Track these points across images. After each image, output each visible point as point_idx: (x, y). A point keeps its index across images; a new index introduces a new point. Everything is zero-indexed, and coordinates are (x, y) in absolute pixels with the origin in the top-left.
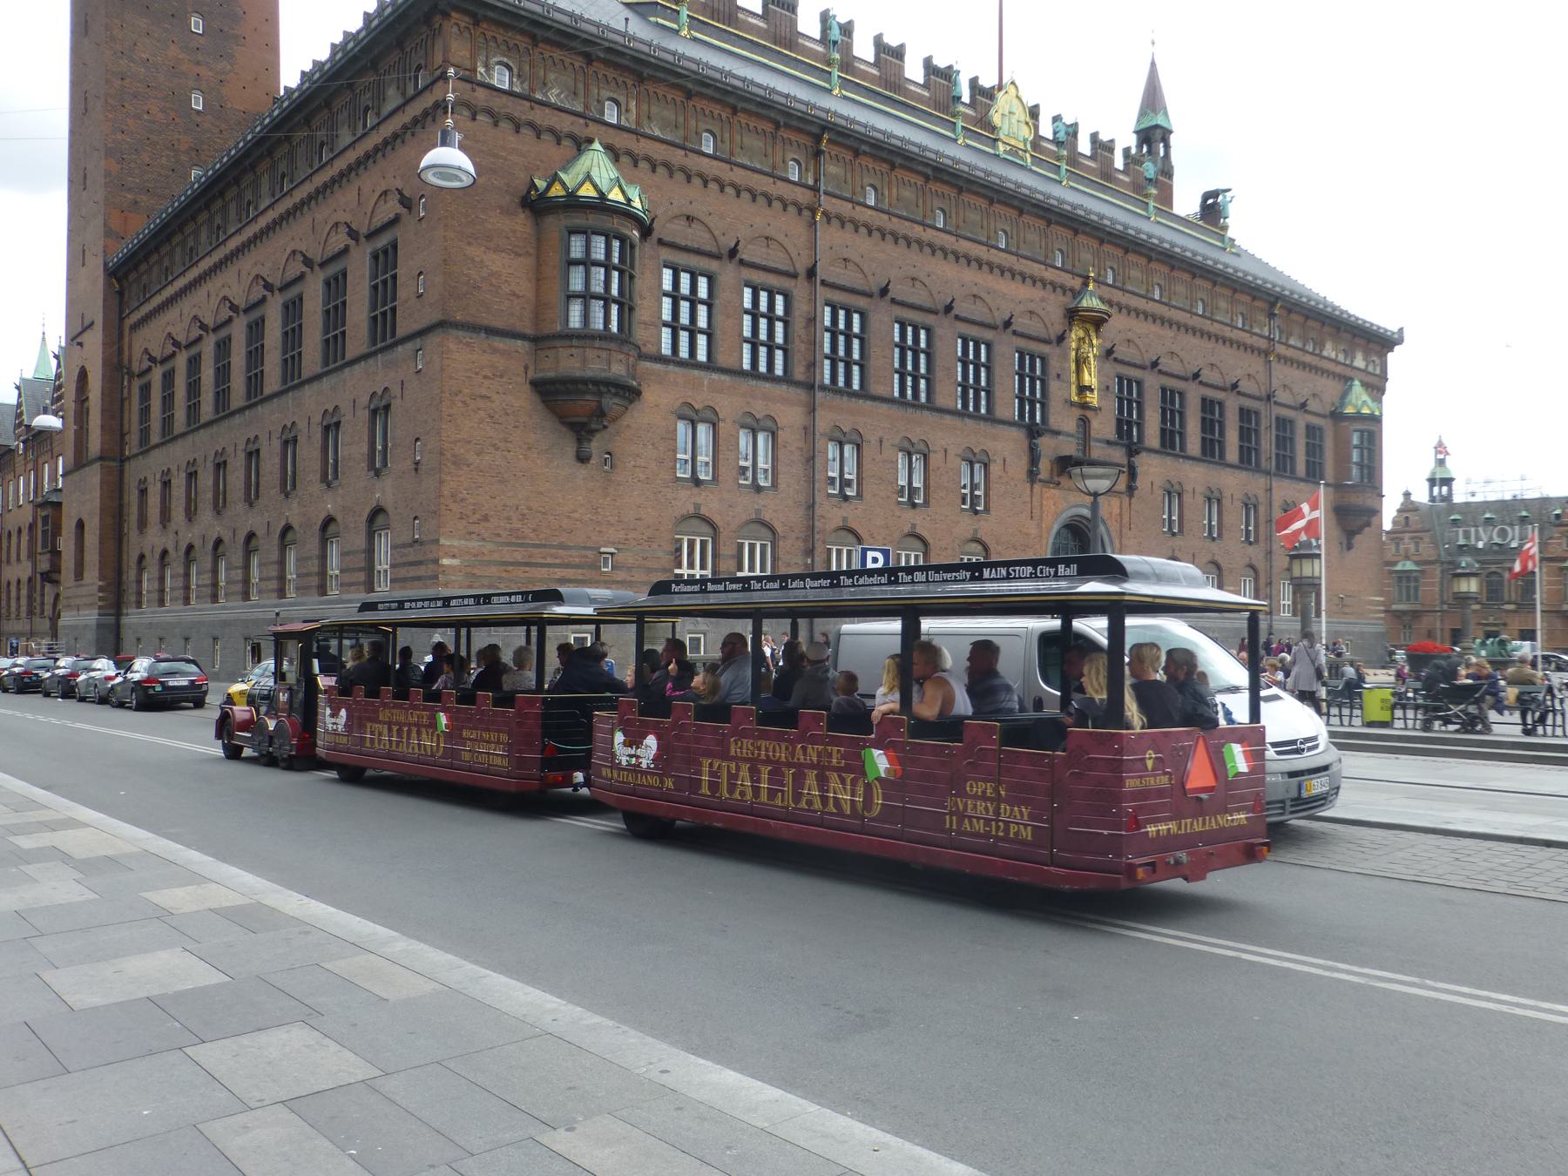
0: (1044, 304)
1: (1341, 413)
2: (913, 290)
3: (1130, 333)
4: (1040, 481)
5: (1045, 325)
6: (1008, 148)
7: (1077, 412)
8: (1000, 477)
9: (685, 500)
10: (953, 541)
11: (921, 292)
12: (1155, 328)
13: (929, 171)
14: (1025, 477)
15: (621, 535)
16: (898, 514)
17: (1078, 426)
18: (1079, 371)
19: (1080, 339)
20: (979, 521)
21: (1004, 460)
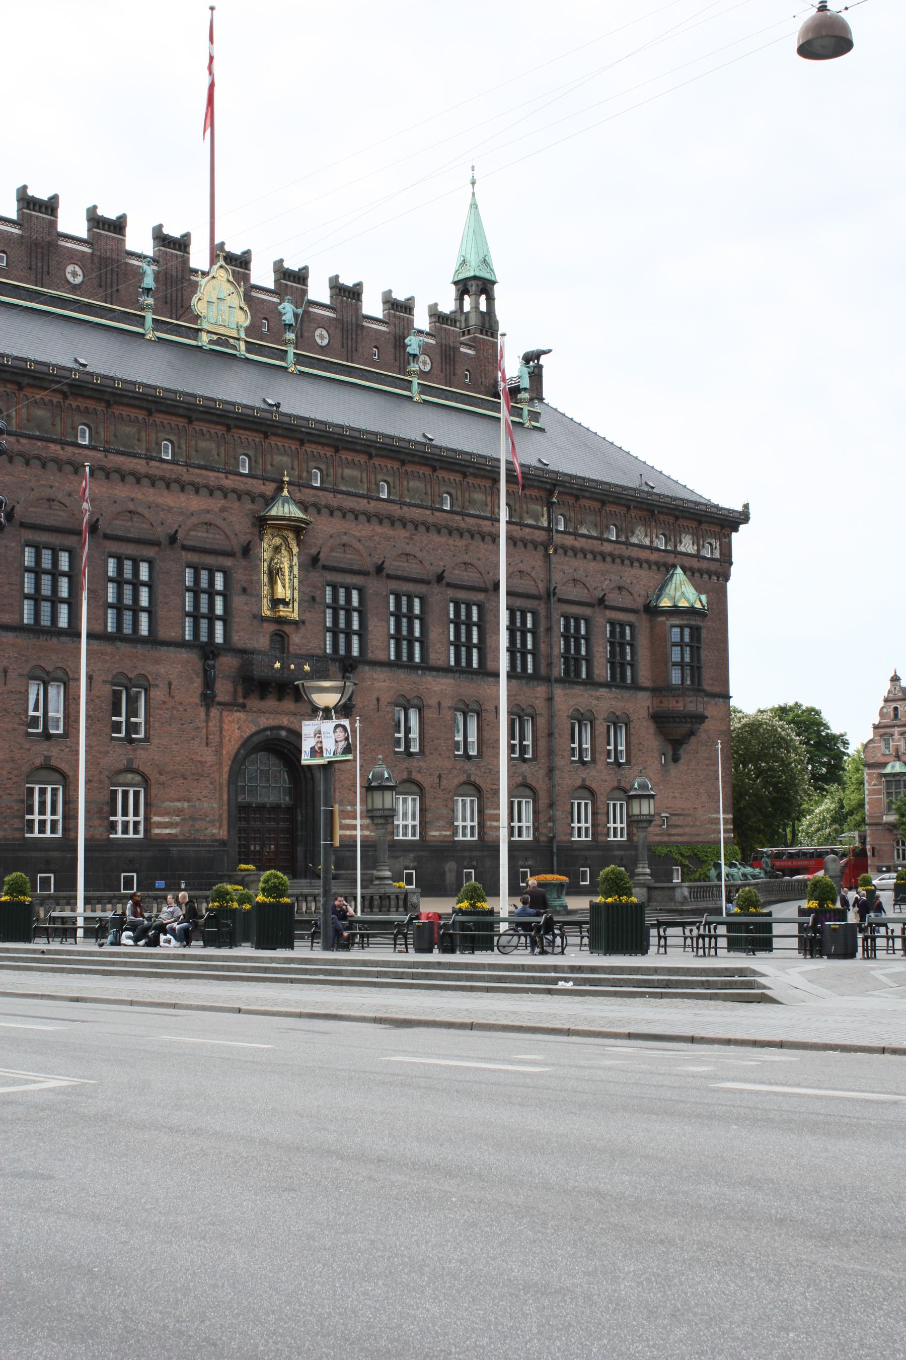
1: (657, 607)
2: (48, 511)
3: (345, 537)
4: (219, 704)
5: (227, 537)
6: (215, 337)
7: (272, 627)
8: (164, 703)
10: (100, 773)
11: (61, 513)
12: (385, 530)
13: (66, 389)
14: (196, 699)
16: (28, 747)
17: (272, 641)
18: (272, 583)
19: (277, 549)
20: (135, 750)
21: (170, 684)
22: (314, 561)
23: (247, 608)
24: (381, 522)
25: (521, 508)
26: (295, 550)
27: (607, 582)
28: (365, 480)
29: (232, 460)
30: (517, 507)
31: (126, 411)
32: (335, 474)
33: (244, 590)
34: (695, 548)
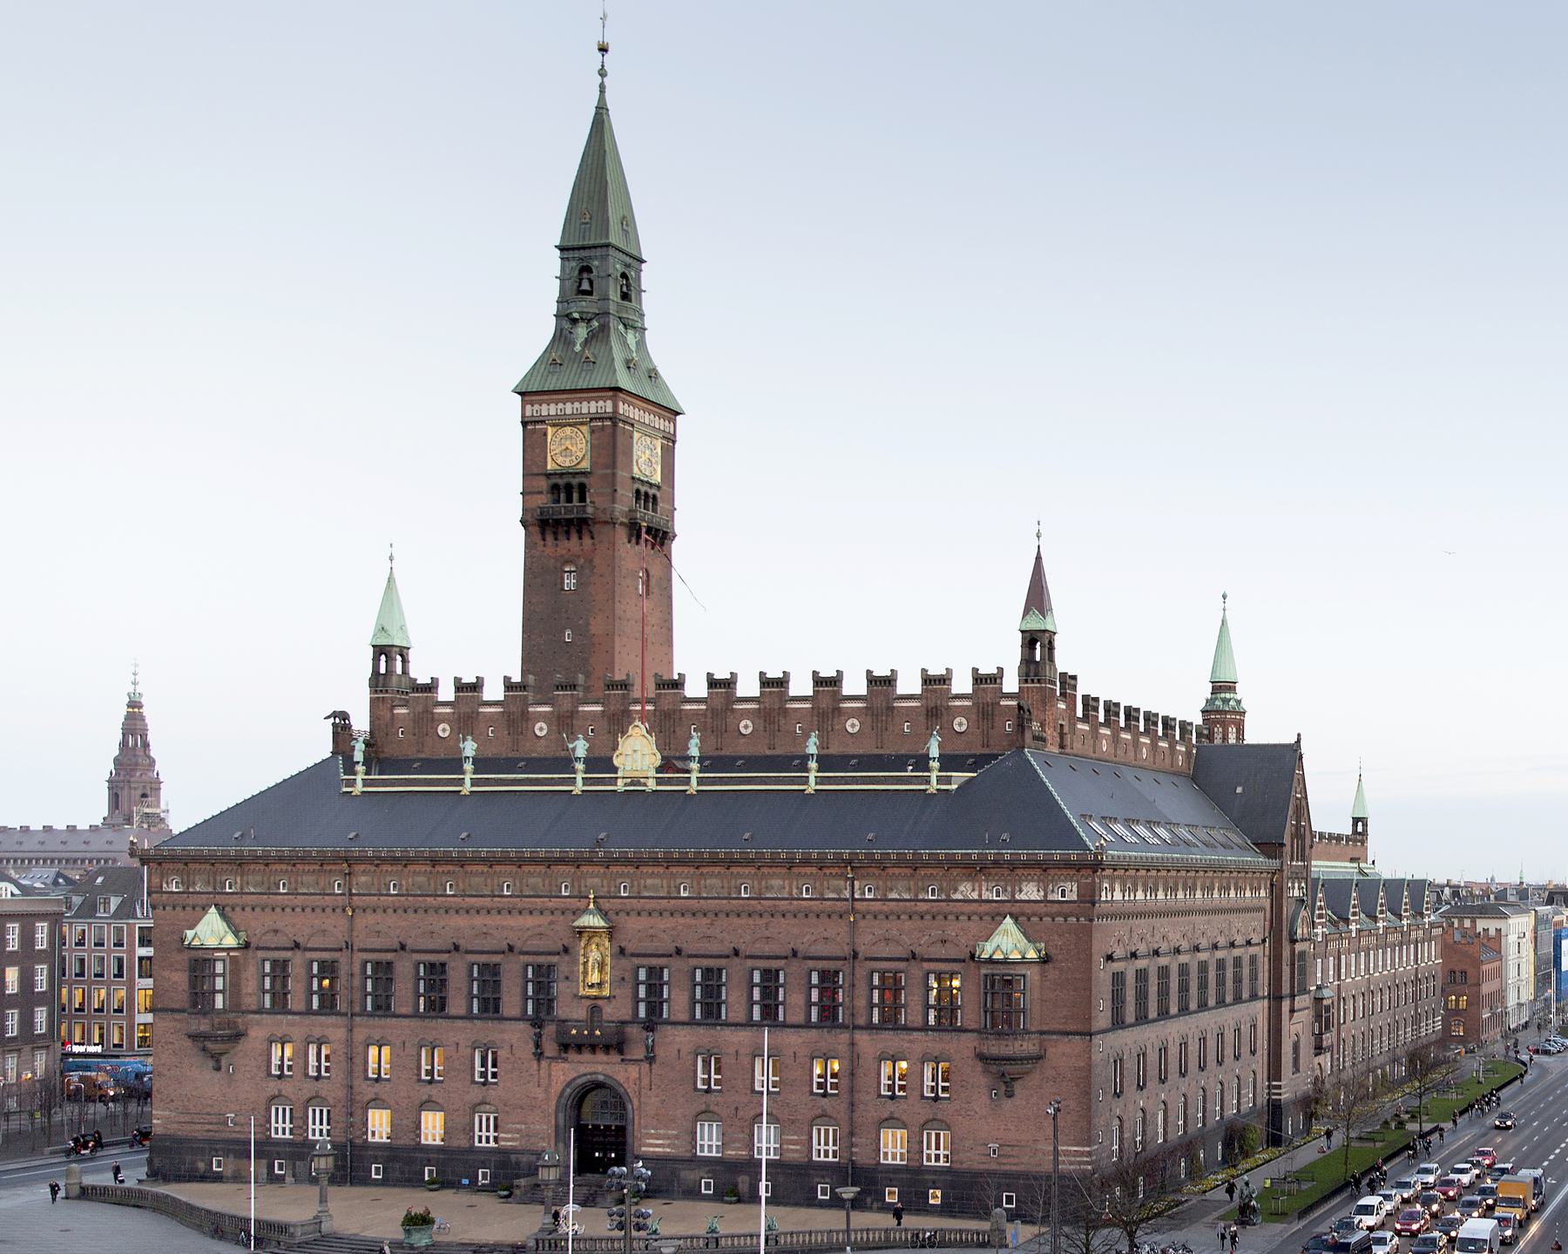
0: (552, 926)
9: (273, 1087)
12: (689, 920)
15: (238, 1107)
22: (622, 951)
23: (568, 990)
24: (683, 915)
25: (822, 885)
26: (607, 944)
27: (927, 937)
28: (665, 885)
29: (555, 888)
30: (818, 884)
31: (475, 868)
32: (639, 885)
33: (567, 978)
34: (1042, 893)
